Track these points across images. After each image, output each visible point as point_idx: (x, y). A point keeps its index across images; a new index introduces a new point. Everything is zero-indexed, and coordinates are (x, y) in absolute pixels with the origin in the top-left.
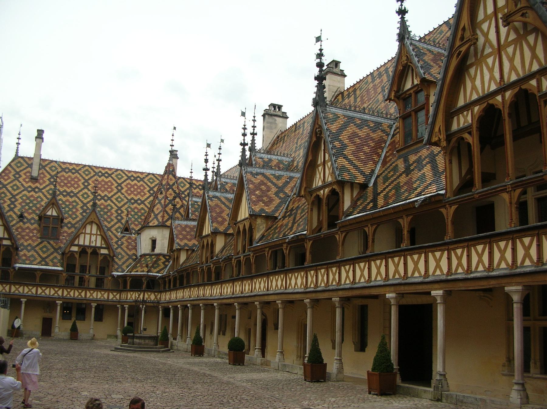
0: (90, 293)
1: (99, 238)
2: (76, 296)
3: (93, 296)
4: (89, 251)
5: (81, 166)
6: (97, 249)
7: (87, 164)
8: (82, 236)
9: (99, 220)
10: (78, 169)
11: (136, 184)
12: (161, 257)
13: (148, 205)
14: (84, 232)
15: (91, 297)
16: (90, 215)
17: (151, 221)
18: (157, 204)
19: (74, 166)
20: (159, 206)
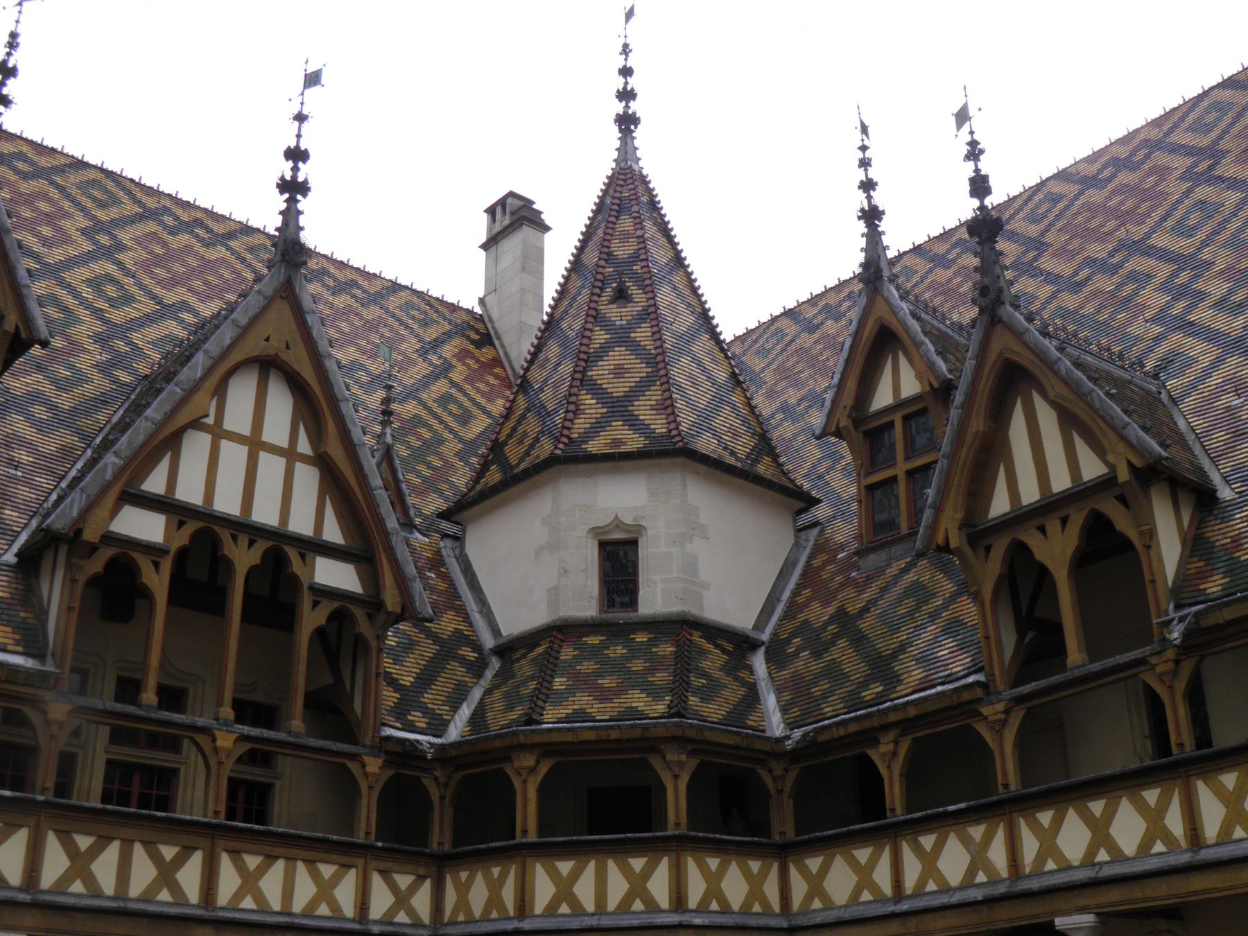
0: (241, 868)
1: (307, 479)
2: (135, 890)
3: (259, 897)
4: (244, 558)
5: (63, 161)
6: (293, 554)
7: (93, 159)
8: (196, 447)
9: (317, 359)
10: (44, 162)
11: (348, 310)
12: (697, 638)
13: (439, 410)
14: (210, 420)
15: (248, 903)
16: (263, 310)
17: (588, 435)
18: (605, 349)
19: (25, 149)
20: (619, 355)
